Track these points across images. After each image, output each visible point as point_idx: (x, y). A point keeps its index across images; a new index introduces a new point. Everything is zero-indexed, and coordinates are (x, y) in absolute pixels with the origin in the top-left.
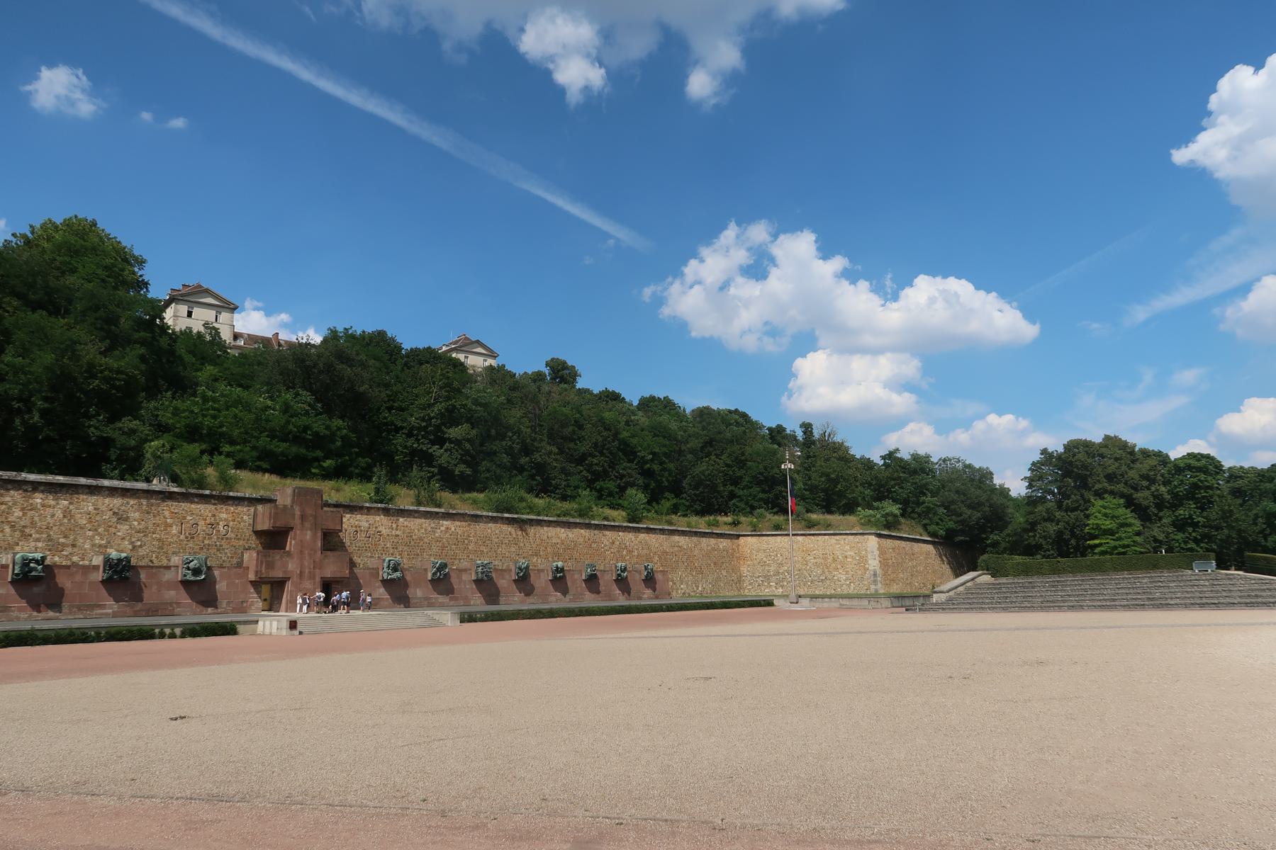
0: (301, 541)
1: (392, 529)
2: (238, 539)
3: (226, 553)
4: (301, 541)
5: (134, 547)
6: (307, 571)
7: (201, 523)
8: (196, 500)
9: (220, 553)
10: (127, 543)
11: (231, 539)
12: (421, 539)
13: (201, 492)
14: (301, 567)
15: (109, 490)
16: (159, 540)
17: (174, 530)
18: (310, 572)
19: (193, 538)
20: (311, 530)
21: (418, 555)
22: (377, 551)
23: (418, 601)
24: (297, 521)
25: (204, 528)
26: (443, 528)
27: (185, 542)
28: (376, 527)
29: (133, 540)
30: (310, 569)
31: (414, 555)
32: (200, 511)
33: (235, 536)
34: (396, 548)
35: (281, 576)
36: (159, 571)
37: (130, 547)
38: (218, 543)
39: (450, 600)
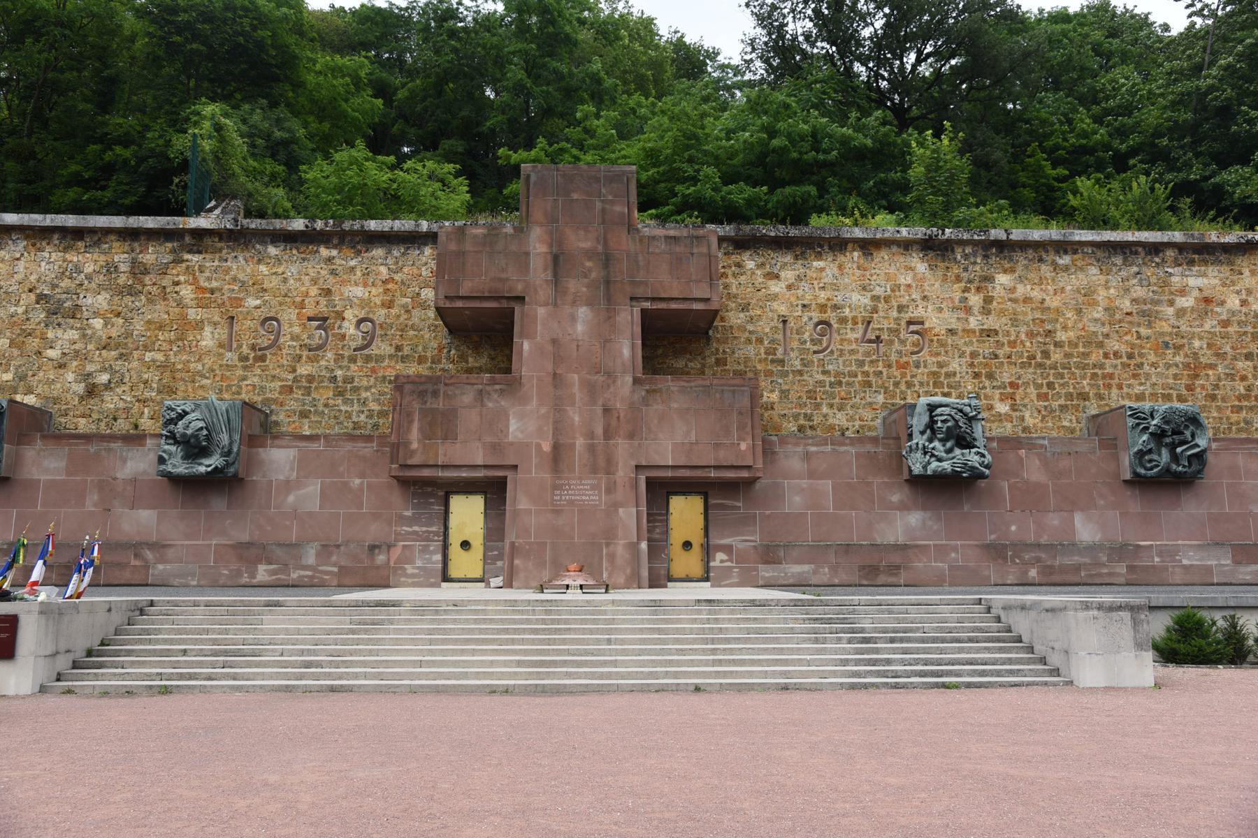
0: (554, 341)
1: (968, 310)
2: (404, 359)
3: (365, 403)
4: (554, 341)
5: (92, 391)
6: (580, 442)
7: (289, 316)
8: (272, 250)
9: (345, 402)
10: (70, 377)
11: (380, 359)
12: (1092, 341)
13: (278, 224)
14: (557, 431)
15: (27, 238)
16: (163, 367)
17: (208, 339)
18: (591, 449)
20: (590, 303)
21: (1084, 397)
23: (1087, 560)
24: (538, 273)
25: (297, 330)
26: (1186, 302)
27: (240, 372)
28: (901, 308)
29: (90, 368)
31: (1069, 396)
32: (285, 280)
34: (990, 376)
36: (109, 450)
37: (80, 388)
38: (339, 373)
39: (1237, 562)
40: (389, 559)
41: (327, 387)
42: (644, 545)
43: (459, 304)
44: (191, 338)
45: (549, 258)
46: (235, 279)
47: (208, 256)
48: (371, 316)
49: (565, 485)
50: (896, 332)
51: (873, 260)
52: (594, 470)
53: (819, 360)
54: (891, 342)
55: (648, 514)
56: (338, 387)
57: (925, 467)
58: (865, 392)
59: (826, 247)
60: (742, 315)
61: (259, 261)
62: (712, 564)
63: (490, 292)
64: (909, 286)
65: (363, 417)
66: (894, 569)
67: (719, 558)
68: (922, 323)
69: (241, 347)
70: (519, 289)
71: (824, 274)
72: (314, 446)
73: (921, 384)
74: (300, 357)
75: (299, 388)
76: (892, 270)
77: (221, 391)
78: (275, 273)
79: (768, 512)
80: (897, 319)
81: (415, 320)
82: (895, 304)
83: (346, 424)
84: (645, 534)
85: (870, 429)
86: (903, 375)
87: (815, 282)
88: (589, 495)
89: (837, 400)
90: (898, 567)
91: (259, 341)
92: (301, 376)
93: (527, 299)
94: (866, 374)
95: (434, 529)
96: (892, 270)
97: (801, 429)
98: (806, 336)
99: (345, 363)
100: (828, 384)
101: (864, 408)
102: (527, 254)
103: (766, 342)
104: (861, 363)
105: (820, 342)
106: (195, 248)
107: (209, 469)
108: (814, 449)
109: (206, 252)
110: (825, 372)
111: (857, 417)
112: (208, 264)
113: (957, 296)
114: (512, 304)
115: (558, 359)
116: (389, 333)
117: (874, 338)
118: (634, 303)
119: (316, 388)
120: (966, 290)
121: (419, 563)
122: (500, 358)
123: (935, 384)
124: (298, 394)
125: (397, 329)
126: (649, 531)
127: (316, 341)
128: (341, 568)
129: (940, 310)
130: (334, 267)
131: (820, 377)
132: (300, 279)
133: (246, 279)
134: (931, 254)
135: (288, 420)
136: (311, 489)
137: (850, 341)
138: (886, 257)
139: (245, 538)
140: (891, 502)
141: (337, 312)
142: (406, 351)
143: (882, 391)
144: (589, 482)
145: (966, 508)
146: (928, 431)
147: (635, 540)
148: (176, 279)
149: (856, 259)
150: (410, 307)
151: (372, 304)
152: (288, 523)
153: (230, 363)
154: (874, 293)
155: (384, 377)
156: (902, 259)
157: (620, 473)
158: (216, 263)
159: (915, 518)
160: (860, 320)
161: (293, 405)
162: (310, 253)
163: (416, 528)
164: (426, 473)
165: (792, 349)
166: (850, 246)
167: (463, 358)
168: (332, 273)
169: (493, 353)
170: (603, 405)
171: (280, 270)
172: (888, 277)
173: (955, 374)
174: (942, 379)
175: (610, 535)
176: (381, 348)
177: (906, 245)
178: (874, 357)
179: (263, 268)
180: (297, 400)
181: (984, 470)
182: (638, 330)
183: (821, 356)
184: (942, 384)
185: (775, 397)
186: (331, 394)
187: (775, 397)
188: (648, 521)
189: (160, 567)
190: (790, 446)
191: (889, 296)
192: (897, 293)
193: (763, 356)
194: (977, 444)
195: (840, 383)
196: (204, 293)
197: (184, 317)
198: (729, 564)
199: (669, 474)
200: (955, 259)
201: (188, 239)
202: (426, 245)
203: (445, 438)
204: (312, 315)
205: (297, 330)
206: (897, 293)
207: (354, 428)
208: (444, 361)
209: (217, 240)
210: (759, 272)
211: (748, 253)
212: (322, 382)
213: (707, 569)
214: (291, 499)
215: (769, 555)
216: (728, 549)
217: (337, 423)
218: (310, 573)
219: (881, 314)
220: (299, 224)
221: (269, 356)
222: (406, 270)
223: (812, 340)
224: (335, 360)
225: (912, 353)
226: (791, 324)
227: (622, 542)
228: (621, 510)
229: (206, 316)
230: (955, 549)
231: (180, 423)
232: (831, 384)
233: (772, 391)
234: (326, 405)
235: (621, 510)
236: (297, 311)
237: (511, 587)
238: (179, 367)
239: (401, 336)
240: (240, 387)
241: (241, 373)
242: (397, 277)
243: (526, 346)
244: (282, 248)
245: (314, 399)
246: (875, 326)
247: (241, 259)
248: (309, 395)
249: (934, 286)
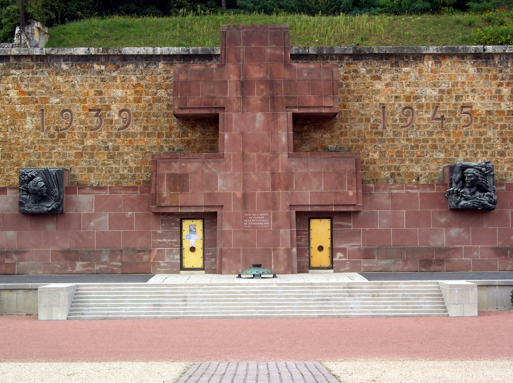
0: (242, 134)
1: (501, 98)
2: (149, 135)
4: (242, 134)
7: (77, 109)
8: (64, 67)
11: (134, 135)
14: (244, 186)
17: (29, 124)
18: (265, 195)
19: (63, 136)
20: (262, 111)
22: (461, 147)
25: (83, 117)
27: (50, 145)
28: (458, 98)
30: (264, 188)
32: (74, 86)
33: (140, 129)
35: (202, 203)
38: (110, 144)
40: (150, 258)
41: (103, 153)
42: (295, 250)
43: (187, 112)
44: (19, 124)
45: (239, 83)
46: (43, 86)
47: (25, 71)
48: (127, 108)
49: (250, 217)
50: (454, 113)
51: (441, 66)
52: (267, 208)
53: (405, 132)
54: (450, 120)
55: (297, 231)
56: (109, 153)
57: (457, 203)
58: (433, 152)
59: (411, 58)
60: (357, 104)
61: (57, 74)
62: (334, 259)
63: (205, 105)
64: (463, 83)
65: (126, 171)
66: (440, 262)
67: (339, 255)
68: (471, 107)
69: (50, 129)
70: (222, 102)
71: (409, 76)
72: (103, 193)
73: (469, 146)
74: (86, 134)
75: (86, 154)
76: (453, 73)
77: (39, 156)
78: (67, 82)
79: (367, 229)
80: (455, 104)
81: (155, 110)
82: (454, 95)
83: (116, 176)
84: (295, 243)
85: (435, 175)
86: (457, 140)
87: (404, 82)
88: (264, 222)
89: (415, 157)
90: (443, 261)
91: (60, 125)
92: (87, 146)
93: (226, 108)
94: (434, 140)
95: (175, 240)
96: (453, 73)
97: (392, 175)
98: (397, 117)
99: (113, 138)
100: (410, 147)
101: (432, 161)
102: (227, 82)
103: (372, 121)
104: (431, 133)
105: (406, 120)
106: (17, 66)
107: (50, 209)
108: (394, 191)
109: (24, 68)
110: (408, 140)
111: (427, 168)
112: (26, 76)
113: (494, 88)
114: (218, 111)
115: (245, 144)
116: (139, 118)
117: (439, 117)
118: (288, 109)
119: (97, 154)
120: (500, 85)
121: (167, 260)
122: (207, 134)
123: (477, 146)
124: (86, 158)
125: (144, 116)
126: (297, 240)
127: (95, 125)
128: (123, 263)
129: (483, 98)
130: (103, 76)
131: (405, 143)
132: (83, 85)
133: (49, 85)
134: (479, 61)
135: (81, 174)
136: (103, 218)
137: (424, 120)
138: (450, 64)
139: (66, 246)
140: (440, 222)
141: (107, 106)
142: (150, 130)
143: (444, 151)
144: (263, 215)
145: (485, 226)
146: (461, 182)
147: (290, 247)
148: (7, 86)
149: (430, 66)
150: (152, 102)
151: (128, 100)
152: (91, 238)
153: (43, 139)
154: (441, 88)
155: (138, 146)
156: (460, 65)
157: (280, 210)
158: (31, 75)
159: (454, 232)
160: (431, 106)
161: (83, 164)
162: (87, 68)
163: (164, 240)
164: (171, 210)
165: (388, 125)
166: (426, 57)
167: (185, 134)
168: (102, 81)
169: (203, 130)
170: (271, 171)
171: (70, 79)
172: (450, 77)
173: (490, 139)
174: (482, 143)
175: (276, 244)
176: (135, 128)
177: (462, 56)
178: (439, 130)
179: (59, 78)
180: (85, 161)
181: (491, 205)
182: (291, 125)
183: (405, 129)
184: (482, 146)
185: (376, 156)
186: (106, 158)
187: (376, 156)
188: (297, 235)
189: (21, 263)
190: (381, 190)
191: (451, 90)
192: (456, 88)
193: (370, 130)
194: (489, 189)
195: (417, 146)
196: (24, 95)
197: (13, 109)
199: (309, 209)
200: (494, 65)
201: (12, 60)
202: (159, 61)
203: (182, 191)
204: (91, 108)
205: (83, 117)
206: (456, 88)
207: (121, 178)
208: (173, 136)
209: (30, 60)
210: (368, 76)
211: (361, 63)
212: (100, 150)
213: (332, 262)
214: (92, 224)
215: (367, 255)
216: (343, 251)
217: (111, 175)
218: (106, 266)
219: (445, 101)
220: (81, 51)
221: (67, 135)
222: (147, 78)
223: (400, 119)
224: (107, 136)
225: (463, 127)
226: (388, 109)
228: (282, 231)
229: (27, 109)
230: (476, 250)
231: (31, 182)
232: (412, 147)
233: (375, 152)
234: (103, 164)
235: (282, 231)
236: (82, 105)
237: (221, 273)
238: (13, 142)
239: (147, 120)
240: (51, 154)
241: (51, 145)
242: (143, 83)
243: (226, 137)
244: (70, 65)
245: (96, 161)
246: (441, 110)
247: (46, 73)
248: (93, 158)
249: (480, 84)
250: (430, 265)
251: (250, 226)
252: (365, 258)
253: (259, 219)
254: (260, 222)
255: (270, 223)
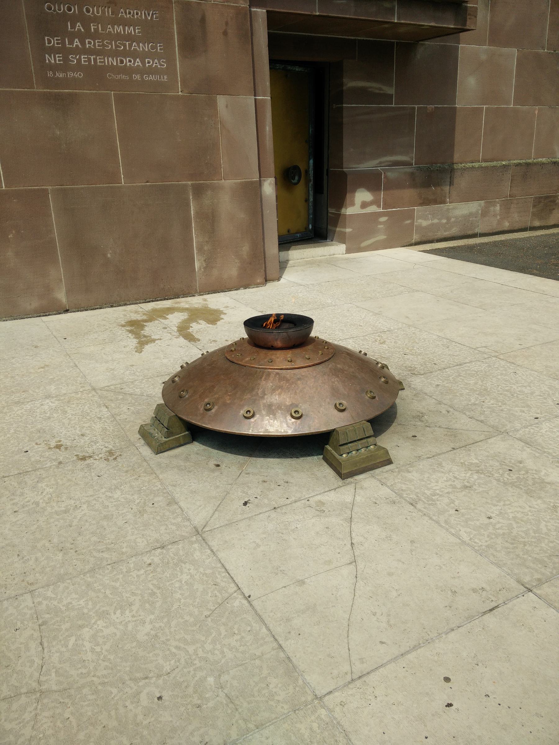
49: (74, 19)
79: (431, 107)
88: (143, 56)
198: (373, 209)
227: (228, 183)
228: (222, 101)
235: (222, 101)
250: (551, 211)
251: (79, 75)
252: (421, 204)
253: (118, 37)
254: (126, 54)
255: (171, 62)
